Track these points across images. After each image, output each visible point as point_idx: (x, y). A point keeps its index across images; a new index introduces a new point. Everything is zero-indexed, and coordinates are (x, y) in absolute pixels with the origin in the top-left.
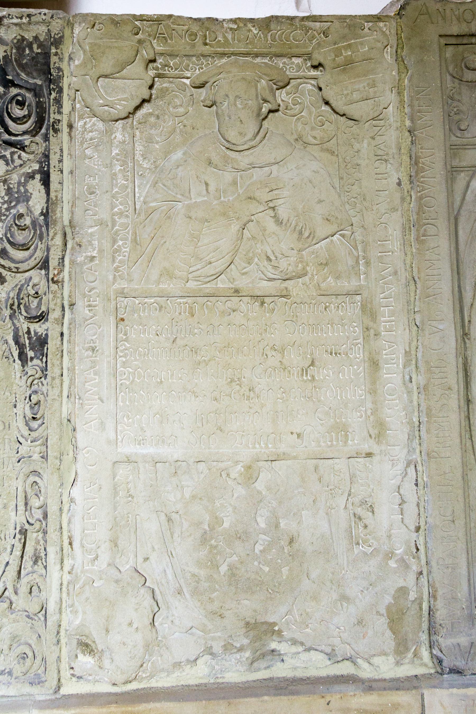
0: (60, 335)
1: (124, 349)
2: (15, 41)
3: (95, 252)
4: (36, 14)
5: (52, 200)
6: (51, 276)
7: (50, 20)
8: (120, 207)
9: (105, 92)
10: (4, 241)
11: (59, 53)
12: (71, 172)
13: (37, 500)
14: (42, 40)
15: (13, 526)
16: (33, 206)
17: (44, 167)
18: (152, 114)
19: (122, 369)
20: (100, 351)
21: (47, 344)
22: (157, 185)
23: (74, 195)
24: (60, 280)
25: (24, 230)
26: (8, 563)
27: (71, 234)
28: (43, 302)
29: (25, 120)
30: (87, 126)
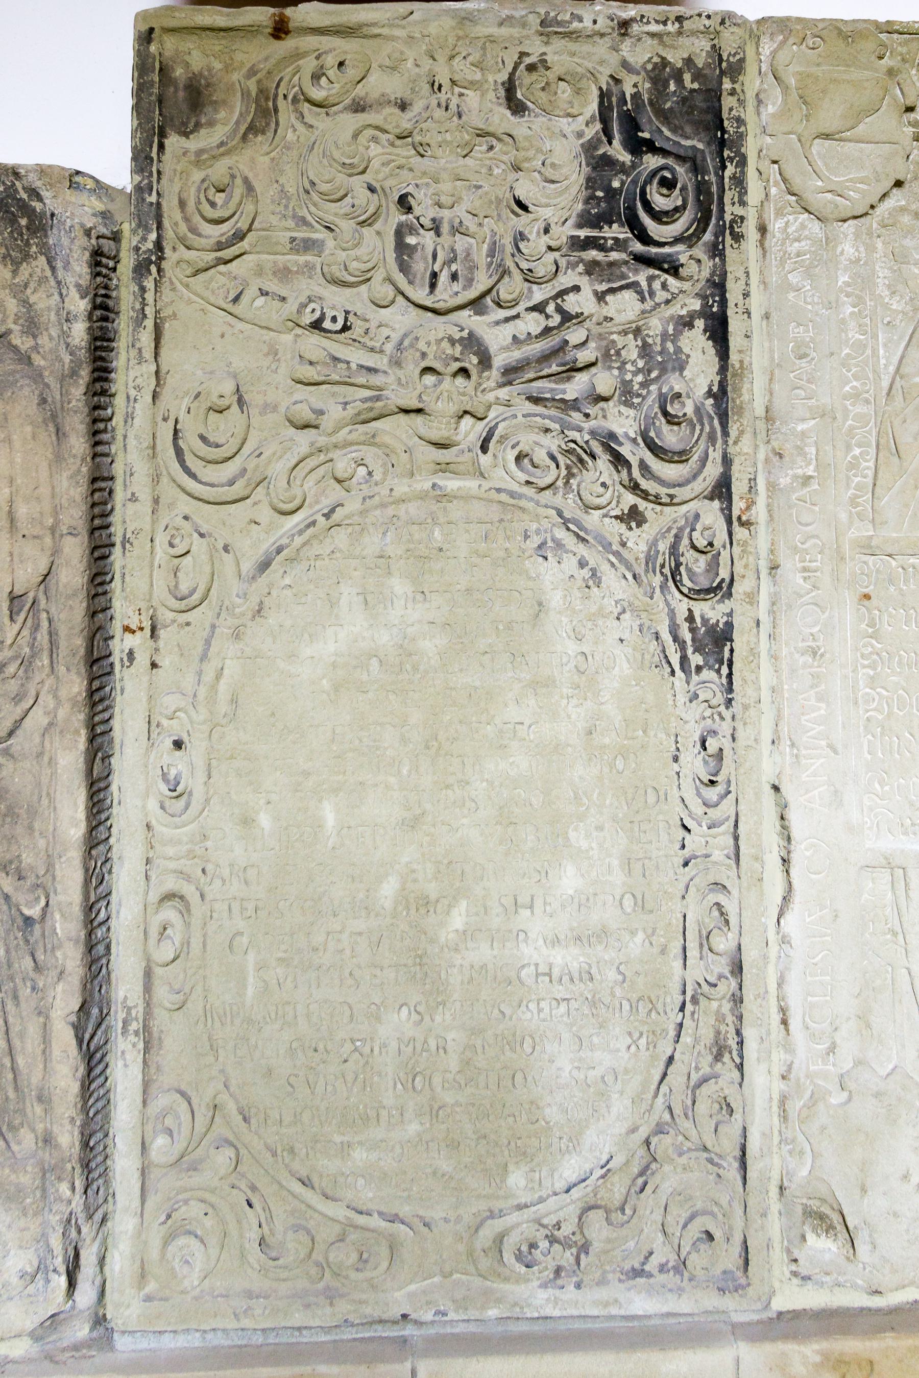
1: (871, 653)
2: (649, 67)
6: (735, 513)
7: (718, 28)
8: (855, 383)
10: (638, 445)
11: (739, 90)
12: (767, 316)
14: (700, 66)
16: (692, 380)
17: (712, 306)
18: (906, 210)
19: (868, 690)
20: (827, 656)
21: (732, 641)
23: (772, 359)
24: (753, 520)
25: (679, 424)
27: (764, 433)
28: (721, 562)
29: (678, 215)
30: (790, 230)
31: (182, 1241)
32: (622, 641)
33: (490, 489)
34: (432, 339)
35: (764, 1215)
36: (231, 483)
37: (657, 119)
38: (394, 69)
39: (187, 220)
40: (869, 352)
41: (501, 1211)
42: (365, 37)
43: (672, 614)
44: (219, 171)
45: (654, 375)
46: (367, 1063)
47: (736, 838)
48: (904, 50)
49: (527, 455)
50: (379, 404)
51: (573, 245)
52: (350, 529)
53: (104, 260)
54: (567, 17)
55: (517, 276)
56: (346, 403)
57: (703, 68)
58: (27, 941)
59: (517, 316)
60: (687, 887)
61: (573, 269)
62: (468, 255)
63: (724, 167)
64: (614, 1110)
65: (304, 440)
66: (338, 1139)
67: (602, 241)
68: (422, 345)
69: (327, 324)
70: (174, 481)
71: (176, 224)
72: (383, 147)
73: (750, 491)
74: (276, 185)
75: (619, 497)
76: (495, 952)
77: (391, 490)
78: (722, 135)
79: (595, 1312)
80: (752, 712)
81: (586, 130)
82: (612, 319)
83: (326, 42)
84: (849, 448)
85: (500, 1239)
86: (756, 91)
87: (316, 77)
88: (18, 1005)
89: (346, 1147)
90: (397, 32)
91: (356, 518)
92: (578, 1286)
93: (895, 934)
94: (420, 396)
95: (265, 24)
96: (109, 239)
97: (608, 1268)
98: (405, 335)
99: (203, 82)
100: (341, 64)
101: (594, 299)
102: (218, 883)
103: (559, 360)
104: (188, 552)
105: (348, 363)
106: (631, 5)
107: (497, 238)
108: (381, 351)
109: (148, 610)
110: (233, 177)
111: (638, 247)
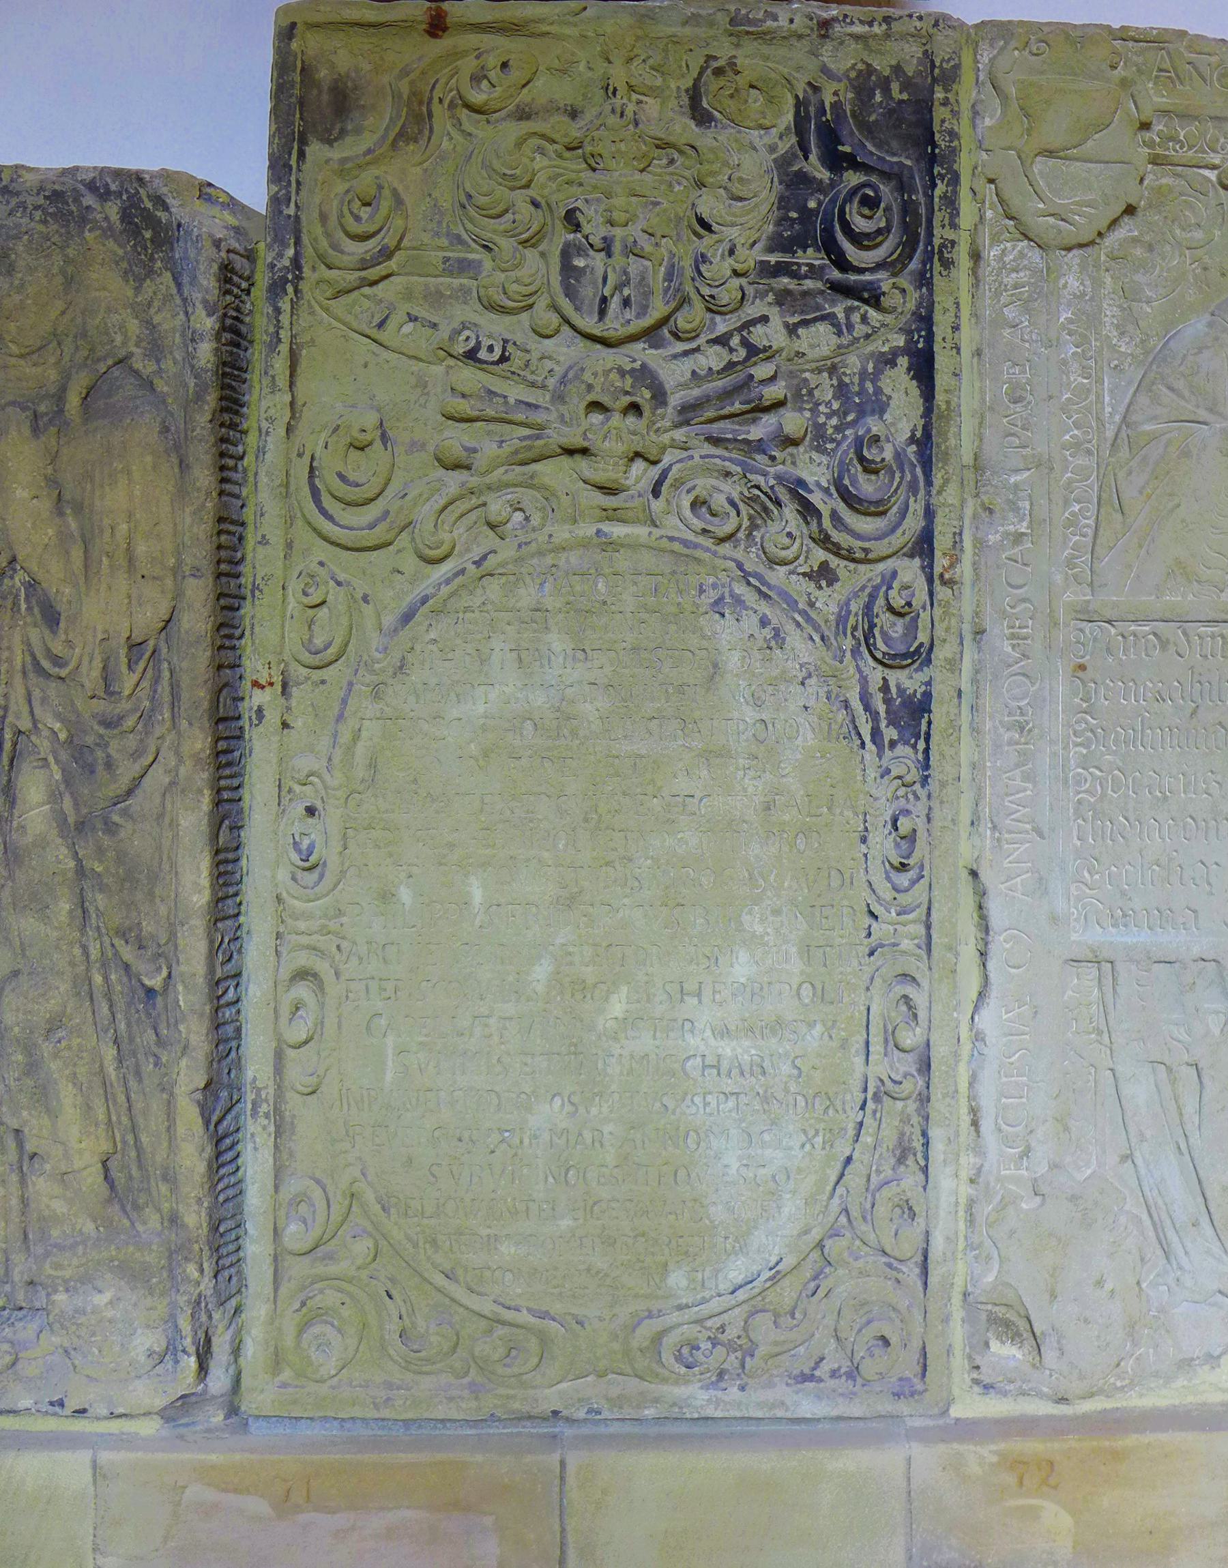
0: (956, 695)
1: (1085, 730)
2: (853, 74)
3: (1025, 524)
4: (901, 17)
5: (939, 409)
6: (937, 570)
7: (931, 31)
9: (1049, 185)
10: (831, 495)
11: (952, 100)
12: (978, 353)
13: (910, 1034)
14: (910, 74)
15: (856, 1085)
16: (893, 424)
18: (1139, 241)
19: (1080, 770)
20: (1036, 731)
21: (930, 712)
22: (1154, 387)
23: (983, 401)
24: (957, 577)
25: (876, 472)
26: (849, 1160)
27: (972, 484)
28: (920, 625)
29: (880, 238)
31: (316, 1329)
32: (806, 708)
33: (662, 537)
34: (600, 370)
35: (946, 1320)
36: (371, 526)
37: (861, 133)
38: (564, 72)
39: (328, 235)
40: (1093, 397)
41: (660, 1311)
42: (532, 35)
43: (864, 681)
44: (366, 181)
45: (850, 418)
46: (516, 1154)
47: (928, 927)
48: (1140, 60)
49: (704, 503)
50: (540, 442)
51: (761, 271)
52: (504, 579)
53: (235, 278)
54: (760, 15)
55: (698, 305)
56: (502, 442)
57: (913, 77)
58: (149, 1015)
59: (697, 349)
60: (872, 979)
61: (762, 299)
62: (643, 279)
63: (934, 185)
64: (786, 1210)
65: (454, 481)
66: (485, 1232)
67: (795, 268)
68: (588, 377)
69: (483, 354)
70: (309, 524)
71: (316, 239)
72: (550, 159)
73: (954, 547)
74: (428, 199)
75: (807, 552)
76: (657, 1043)
77: (550, 536)
78: (933, 150)
79: (759, 1414)
80: (950, 789)
81: (779, 143)
82: (804, 354)
83: (487, 40)
84: (1066, 503)
85: (658, 1338)
86: (972, 102)
87: (476, 79)
88: (140, 1081)
89: (492, 1240)
90: (567, 31)
91: (510, 566)
92: (742, 1388)
93: (1100, 1033)
94: (585, 433)
95: (420, 19)
96: (242, 256)
97: (775, 1372)
98: (571, 368)
99: (349, 84)
100: (505, 65)
101: (784, 331)
102: (354, 961)
103: (743, 398)
104: (324, 602)
105: (505, 397)
106: (834, 6)
107: (676, 259)
108: (544, 387)
109: (279, 664)
110: (380, 187)
111: (836, 274)
